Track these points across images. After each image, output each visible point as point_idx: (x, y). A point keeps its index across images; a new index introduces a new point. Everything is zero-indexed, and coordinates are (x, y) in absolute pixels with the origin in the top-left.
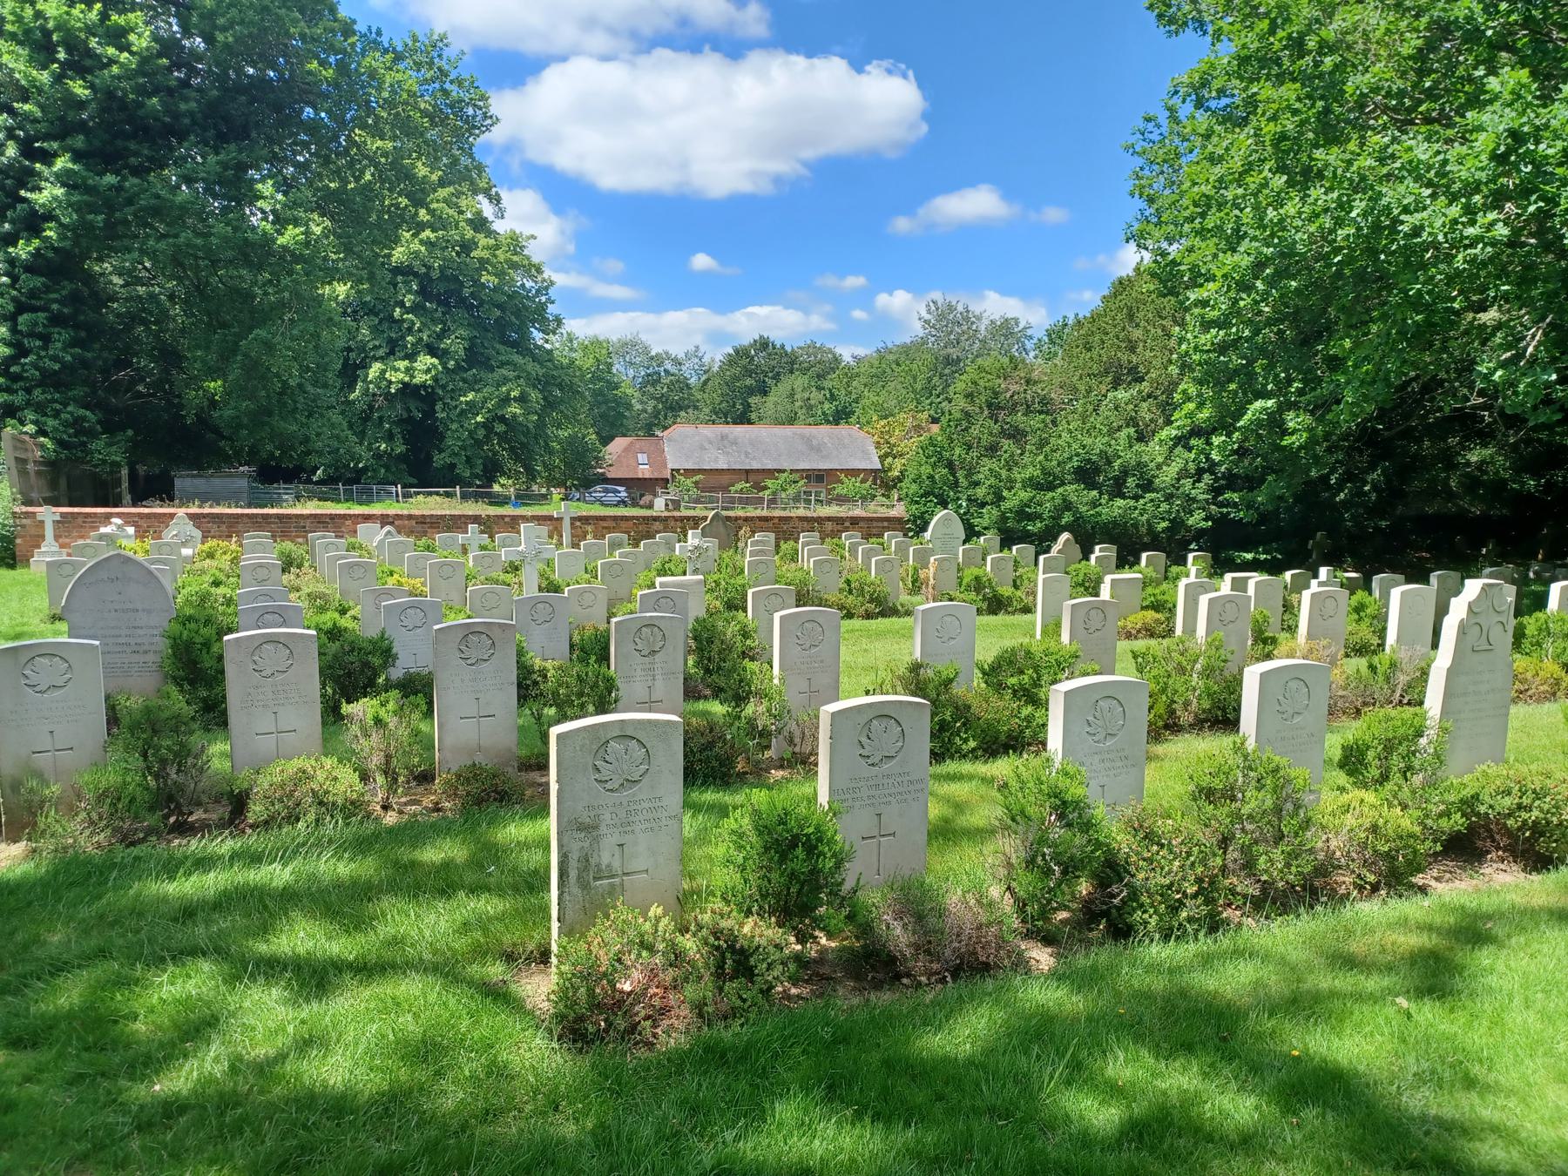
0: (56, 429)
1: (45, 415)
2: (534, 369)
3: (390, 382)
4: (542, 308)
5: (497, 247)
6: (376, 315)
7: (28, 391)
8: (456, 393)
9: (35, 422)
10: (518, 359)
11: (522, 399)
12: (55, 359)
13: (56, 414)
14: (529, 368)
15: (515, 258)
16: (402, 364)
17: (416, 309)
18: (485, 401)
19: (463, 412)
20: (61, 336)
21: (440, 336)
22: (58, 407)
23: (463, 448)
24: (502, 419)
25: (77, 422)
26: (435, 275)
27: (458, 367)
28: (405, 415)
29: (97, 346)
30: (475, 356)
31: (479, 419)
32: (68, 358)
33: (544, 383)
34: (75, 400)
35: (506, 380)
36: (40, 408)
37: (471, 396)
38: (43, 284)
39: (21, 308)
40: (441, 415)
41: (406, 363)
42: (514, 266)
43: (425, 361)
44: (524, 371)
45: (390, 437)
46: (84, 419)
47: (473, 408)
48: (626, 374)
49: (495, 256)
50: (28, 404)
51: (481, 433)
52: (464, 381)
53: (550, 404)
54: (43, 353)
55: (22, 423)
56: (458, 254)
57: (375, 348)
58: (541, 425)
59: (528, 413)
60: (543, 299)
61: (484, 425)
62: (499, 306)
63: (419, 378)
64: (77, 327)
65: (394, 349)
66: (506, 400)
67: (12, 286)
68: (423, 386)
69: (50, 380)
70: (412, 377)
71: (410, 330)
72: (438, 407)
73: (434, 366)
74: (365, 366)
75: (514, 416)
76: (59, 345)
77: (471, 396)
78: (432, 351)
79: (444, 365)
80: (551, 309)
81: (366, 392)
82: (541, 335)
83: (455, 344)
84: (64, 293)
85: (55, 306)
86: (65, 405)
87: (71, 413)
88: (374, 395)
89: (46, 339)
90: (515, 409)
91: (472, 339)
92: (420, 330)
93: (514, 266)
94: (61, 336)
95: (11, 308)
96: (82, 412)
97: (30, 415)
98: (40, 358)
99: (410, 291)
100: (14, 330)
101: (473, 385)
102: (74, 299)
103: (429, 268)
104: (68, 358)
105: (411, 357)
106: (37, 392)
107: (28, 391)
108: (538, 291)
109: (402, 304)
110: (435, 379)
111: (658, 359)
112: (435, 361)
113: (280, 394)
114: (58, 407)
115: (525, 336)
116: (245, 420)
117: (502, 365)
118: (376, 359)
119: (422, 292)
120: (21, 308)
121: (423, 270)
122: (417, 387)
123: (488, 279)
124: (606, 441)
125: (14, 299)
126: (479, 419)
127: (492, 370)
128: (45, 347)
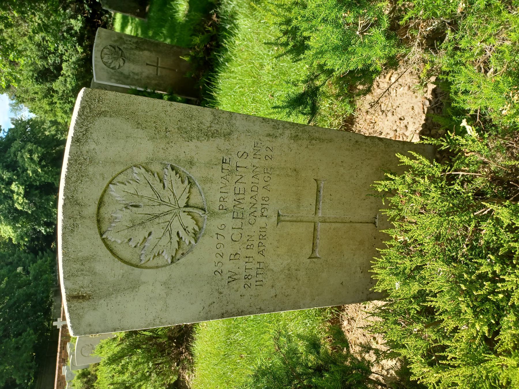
3: (24, 201)
10: (13, 150)
11: (31, 152)
14: (16, 146)
16: (15, 197)
23: (52, 177)
24: (40, 162)
30: (12, 166)
31: (40, 170)
33: (25, 142)
35: (22, 156)
37: (30, 172)
40: (38, 184)
43: (14, 187)
45: (48, 200)
47: (35, 172)
52: (23, 172)
57: (7, 202)
63: (22, 190)
65: (9, 197)
66: (31, 159)
68: (25, 190)
70: (21, 193)
72: (35, 184)
73: (16, 185)
74: (16, 209)
75: (38, 157)
77: (30, 172)
81: (29, 209)
82: (2, 132)
83: (6, 175)
90: (35, 157)
101: (25, 170)
105: (13, 192)
110: (22, 185)
112: (14, 183)
117: (15, 155)
118: (13, 205)
122: (26, 192)
126: (40, 170)
127: (16, 162)
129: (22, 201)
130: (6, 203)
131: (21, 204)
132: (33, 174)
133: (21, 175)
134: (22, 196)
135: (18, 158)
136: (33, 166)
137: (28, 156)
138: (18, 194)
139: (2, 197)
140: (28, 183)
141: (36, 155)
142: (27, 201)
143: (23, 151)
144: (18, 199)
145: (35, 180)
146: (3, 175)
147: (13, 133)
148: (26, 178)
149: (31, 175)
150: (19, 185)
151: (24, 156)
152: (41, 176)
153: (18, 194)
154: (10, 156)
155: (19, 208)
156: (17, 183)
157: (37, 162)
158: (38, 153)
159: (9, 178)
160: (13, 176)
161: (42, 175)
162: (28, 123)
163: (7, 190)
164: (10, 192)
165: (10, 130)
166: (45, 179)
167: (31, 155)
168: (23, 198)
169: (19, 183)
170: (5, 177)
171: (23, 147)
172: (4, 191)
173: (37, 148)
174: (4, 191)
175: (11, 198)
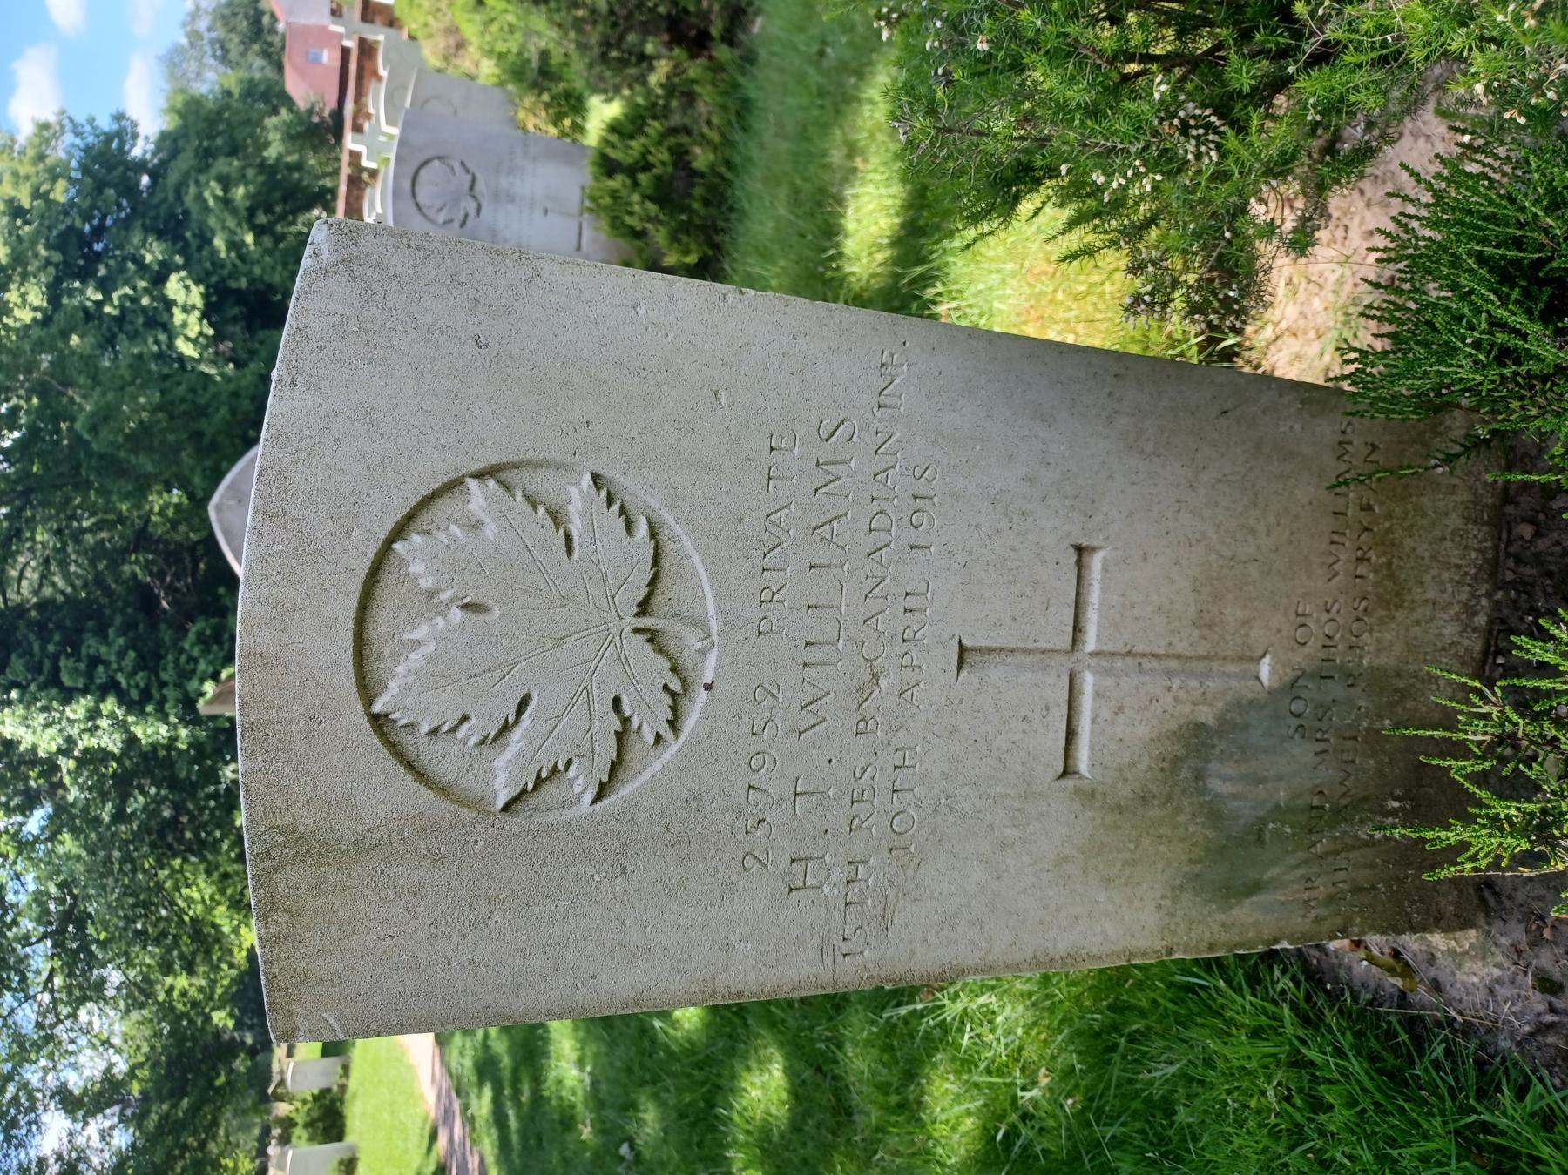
0: (211, 662)
1: (194, 671)
2: (185, 161)
3: (201, 333)
4: (109, 138)
5: (15, 174)
6: (114, 336)
7: (163, 685)
8: (217, 264)
9: (202, 681)
10: (173, 178)
11: (226, 182)
12: (121, 654)
13: (196, 661)
15: (31, 153)
16: (178, 317)
17: (106, 286)
18: (224, 228)
19: (241, 257)
20: (91, 645)
21: (142, 266)
22: (183, 658)
24: (251, 212)
25: (201, 639)
26: (57, 257)
27: (182, 252)
28: (243, 323)
29: (107, 612)
31: (249, 238)
32: (121, 641)
33: (206, 156)
34: (176, 641)
35: (199, 197)
36: (185, 675)
38: (21, 656)
39: (54, 681)
40: (243, 283)
41: (176, 311)
42: (41, 157)
43: (174, 287)
44: (187, 175)
46: (200, 634)
47: (233, 245)
48: (211, 81)
49: (27, 178)
50: (178, 686)
51: (267, 241)
52: (200, 248)
53: (234, 150)
54: (114, 666)
55: (203, 694)
56: (27, 223)
57: (157, 342)
58: (262, 167)
59: (243, 179)
60: (88, 128)
61: (257, 236)
62: (100, 187)
63: (196, 296)
64: (80, 631)
65: (159, 319)
66: (226, 202)
67: (23, 688)
68: (206, 296)
69: (149, 661)
70: (194, 307)
71: (134, 300)
72: (233, 284)
73: (182, 279)
74: (181, 359)
75: (247, 196)
76: (103, 649)
77: (219, 242)
78: (160, 279)
79: (178, 269)
80: (106, 124)
81: (214, 362)
82: (140, 142)
83: (153, 253)
84: (32, 637)
85: (51, 648)
86: (182, 651)
87: (192, 646)
88: (217, 353)
89: (95, 661)
90: (240, 192)
91: (147, 230)
92: (134, 288)
93: (41, 157)
94: (91, 645)
95: (54, 691)
96: (192, 636)
97: (192, 685)
98: (120, 669)
99: (82, 292)
100: (85, 691)
101: (205, 239)
102: (42, 629)
103: (48, 262)
104: (121, 641)
105: (169, 304)
106: (164, 676)
107: (163, 685)
108: (77, 134)
109: (99, 304)
110: (197, 282)
111: (194, 36)
112: (174, 278)
113: (172, 417)
114: (183, 658)
115: (141, 166)
116: (208, 463)
117: (179, 197)
118: (171, 345)
119: (85, 275)
120: (54, 681)
121: (52, 270)
123: (61, 193)
124: (288, 101)
125: (42, 687)
127: (186, 213)
128: (106, 663)
129: (197, 329)
130: (151, 340)
131: (194, 341)
132: (229, 249)
133: (196, 256)
134: (197, 314)
135: (188, 200)
136: (231, 223)
137: (220, 193)
138: (186, 309)
139: (141, 320)
140: (214, 279)
141: (241, 191)
142: (211, 332)
143: (202, 178)
144: (185, 325)
145: (234, 275)
146: (143, 252)
147: (175, 141)
148: (208, 265)
149: (223, 255)
150: (189, 282)
151: (207, 194)
152: (252, 263)
153: (186, 309)
154: (165, 200)
155: (188, 350)
156: (183, 273)
157: (244, 214)
158: (246, 185)
159: (162, 264)
160: (171, 257)
161: (256, 256)
162: (220, 112)
163: (153, 299)
164: (161, 306)
165: (164, 136)
166: (263, 270)
167: (226, 190)
168: (200, 320)
169: (190, 276)
170: (149, 258)
171: (204, 168)
172: (145, 301)
173: (244, 176)
174: (145, 301)
175: (166, 327)
